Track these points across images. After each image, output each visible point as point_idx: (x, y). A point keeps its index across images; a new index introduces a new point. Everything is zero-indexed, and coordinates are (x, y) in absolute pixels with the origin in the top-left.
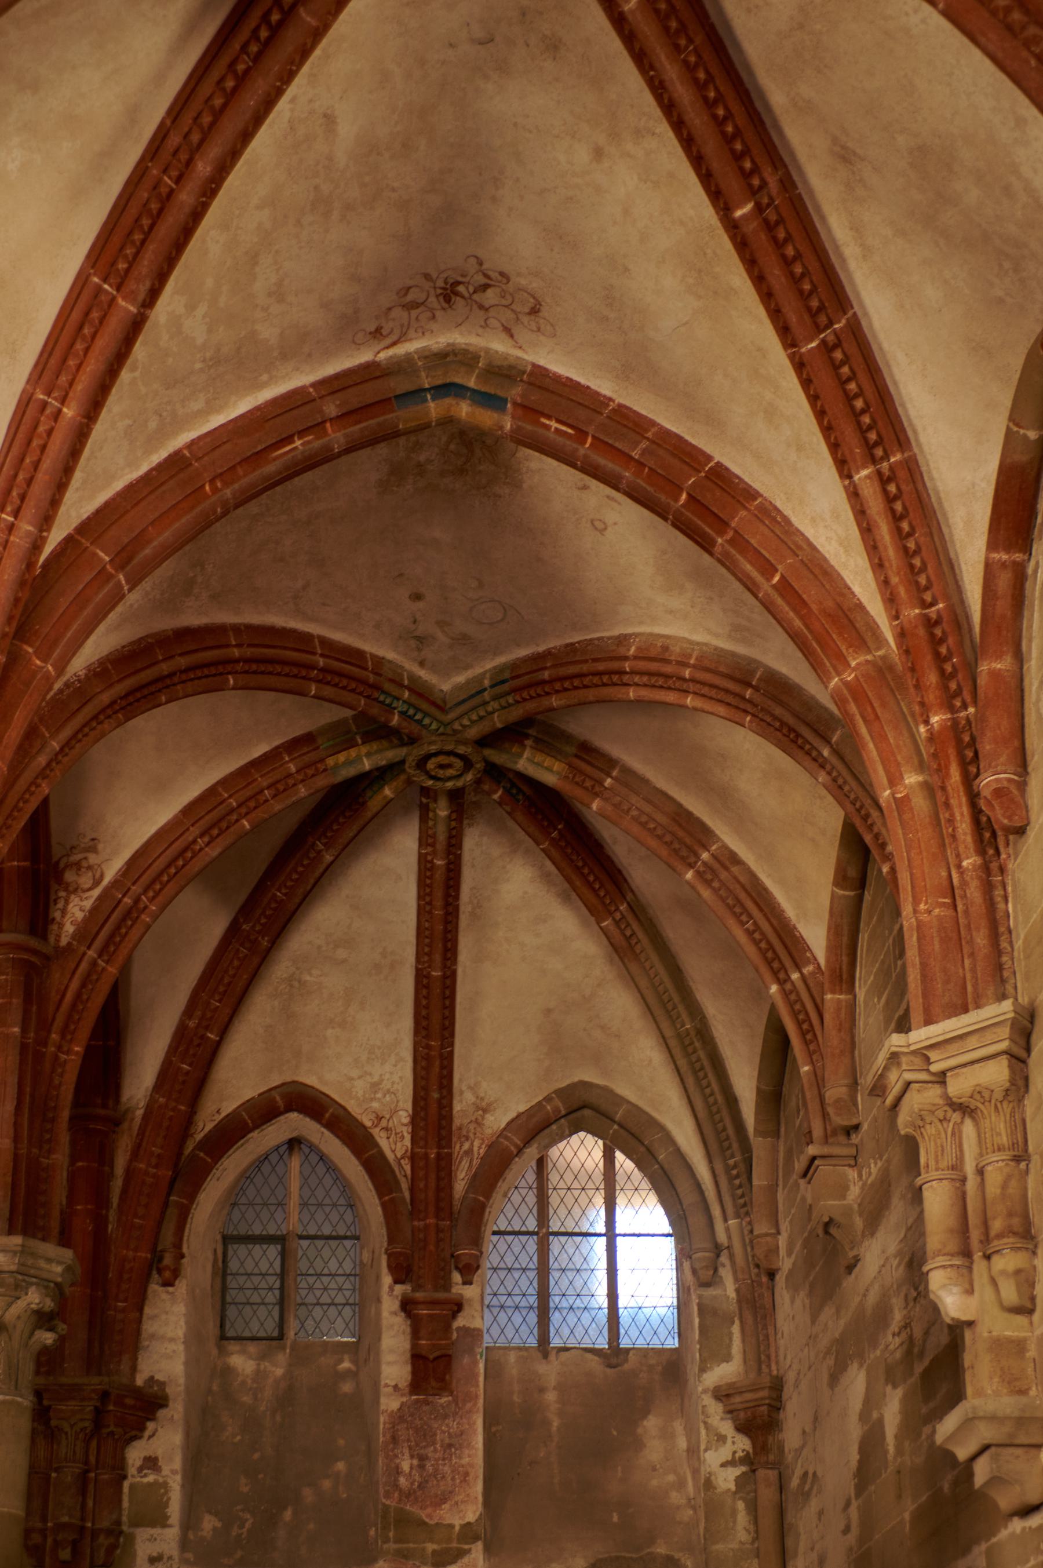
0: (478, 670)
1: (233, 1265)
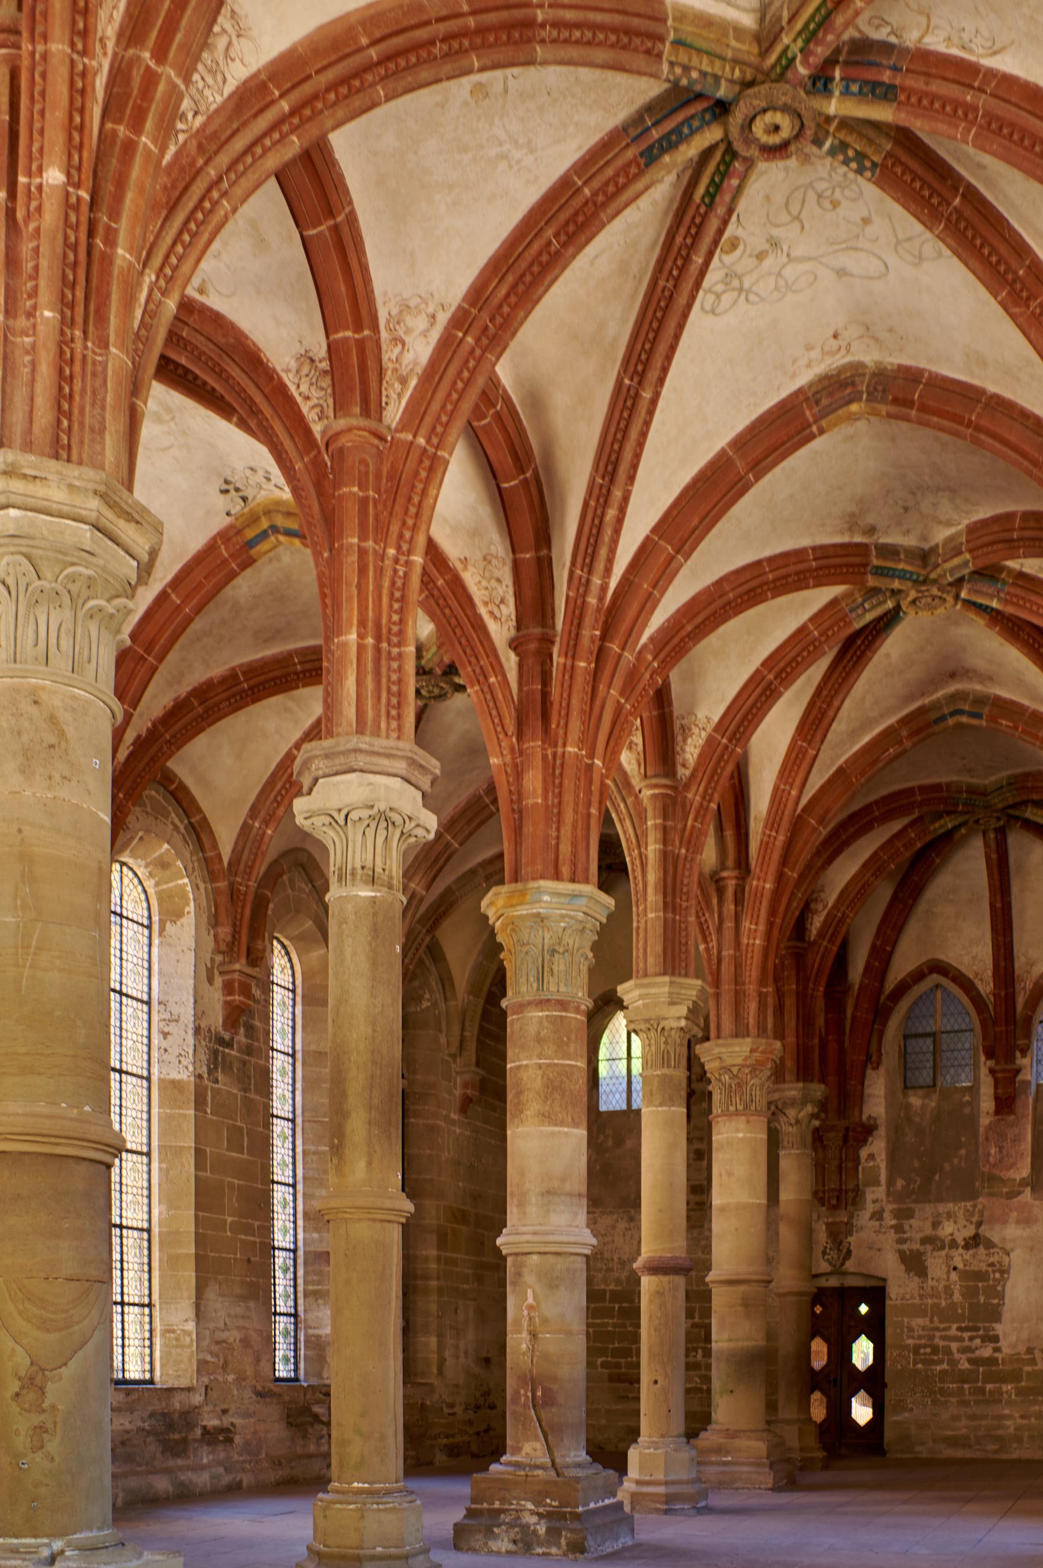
1: (909, 1050)
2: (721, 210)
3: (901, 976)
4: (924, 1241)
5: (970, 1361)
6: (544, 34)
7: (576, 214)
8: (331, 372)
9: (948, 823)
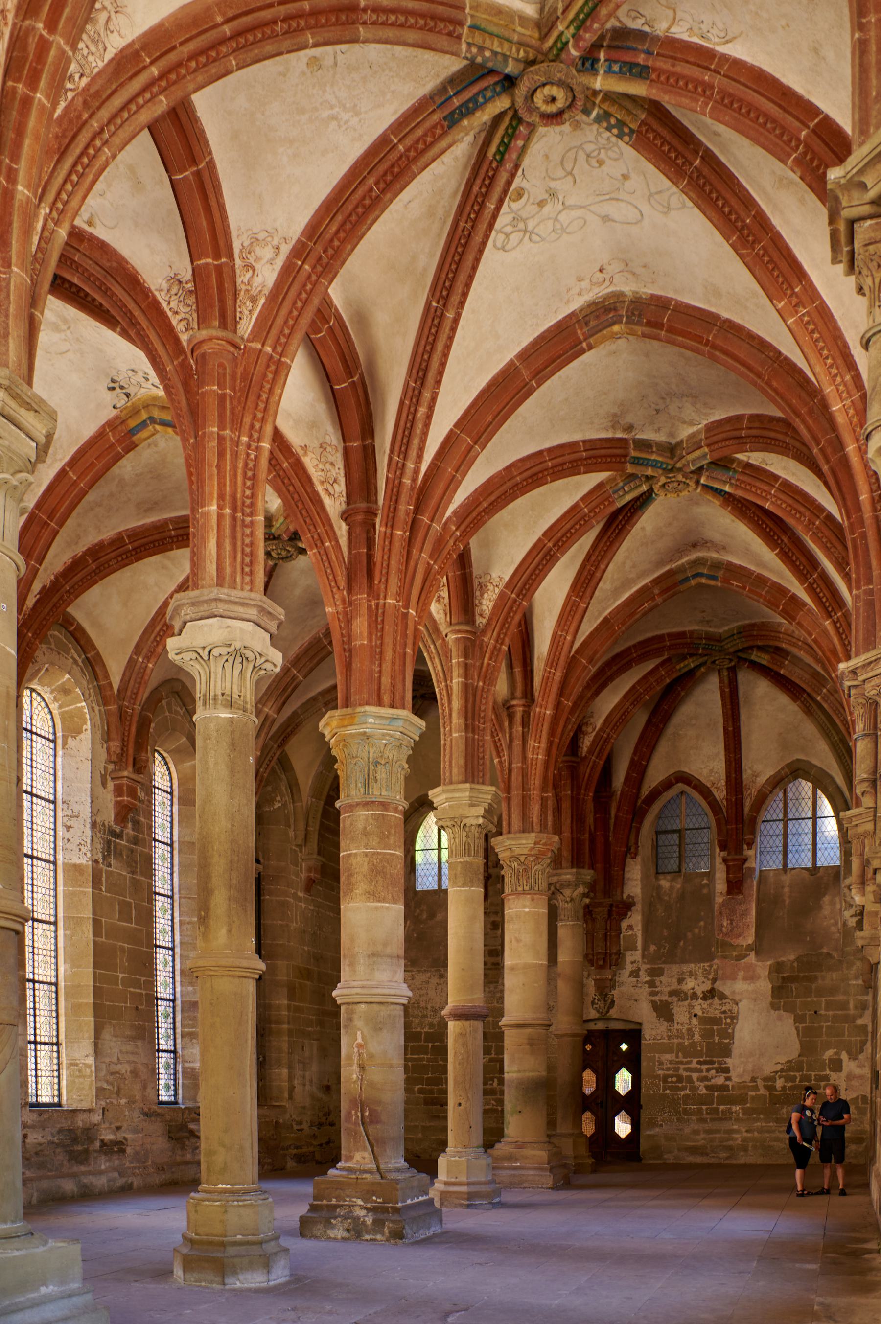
0: (731, 626)
1: (660, 843)
2: (509, 166)
3: (654, 785)
4: (672, 993)
5: (707, 1087)
6: (367, 16)
7: (393, 166)
8: (195, 292)
9: (691, 663)
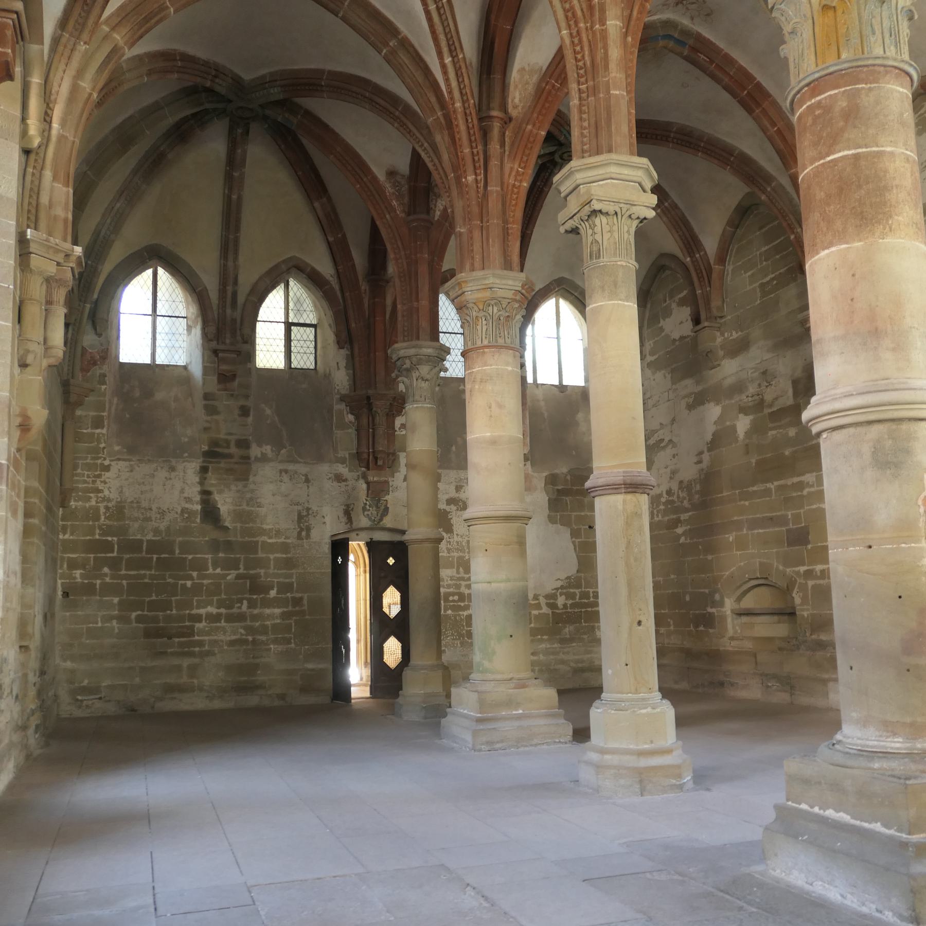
4: (450, 501)
